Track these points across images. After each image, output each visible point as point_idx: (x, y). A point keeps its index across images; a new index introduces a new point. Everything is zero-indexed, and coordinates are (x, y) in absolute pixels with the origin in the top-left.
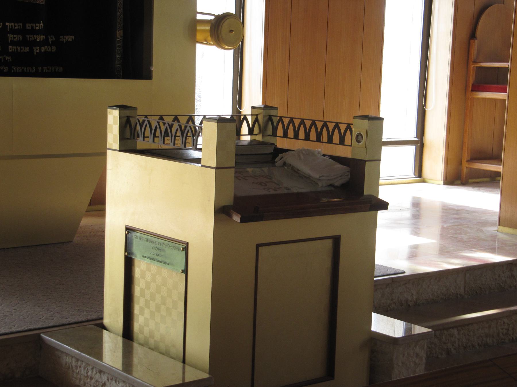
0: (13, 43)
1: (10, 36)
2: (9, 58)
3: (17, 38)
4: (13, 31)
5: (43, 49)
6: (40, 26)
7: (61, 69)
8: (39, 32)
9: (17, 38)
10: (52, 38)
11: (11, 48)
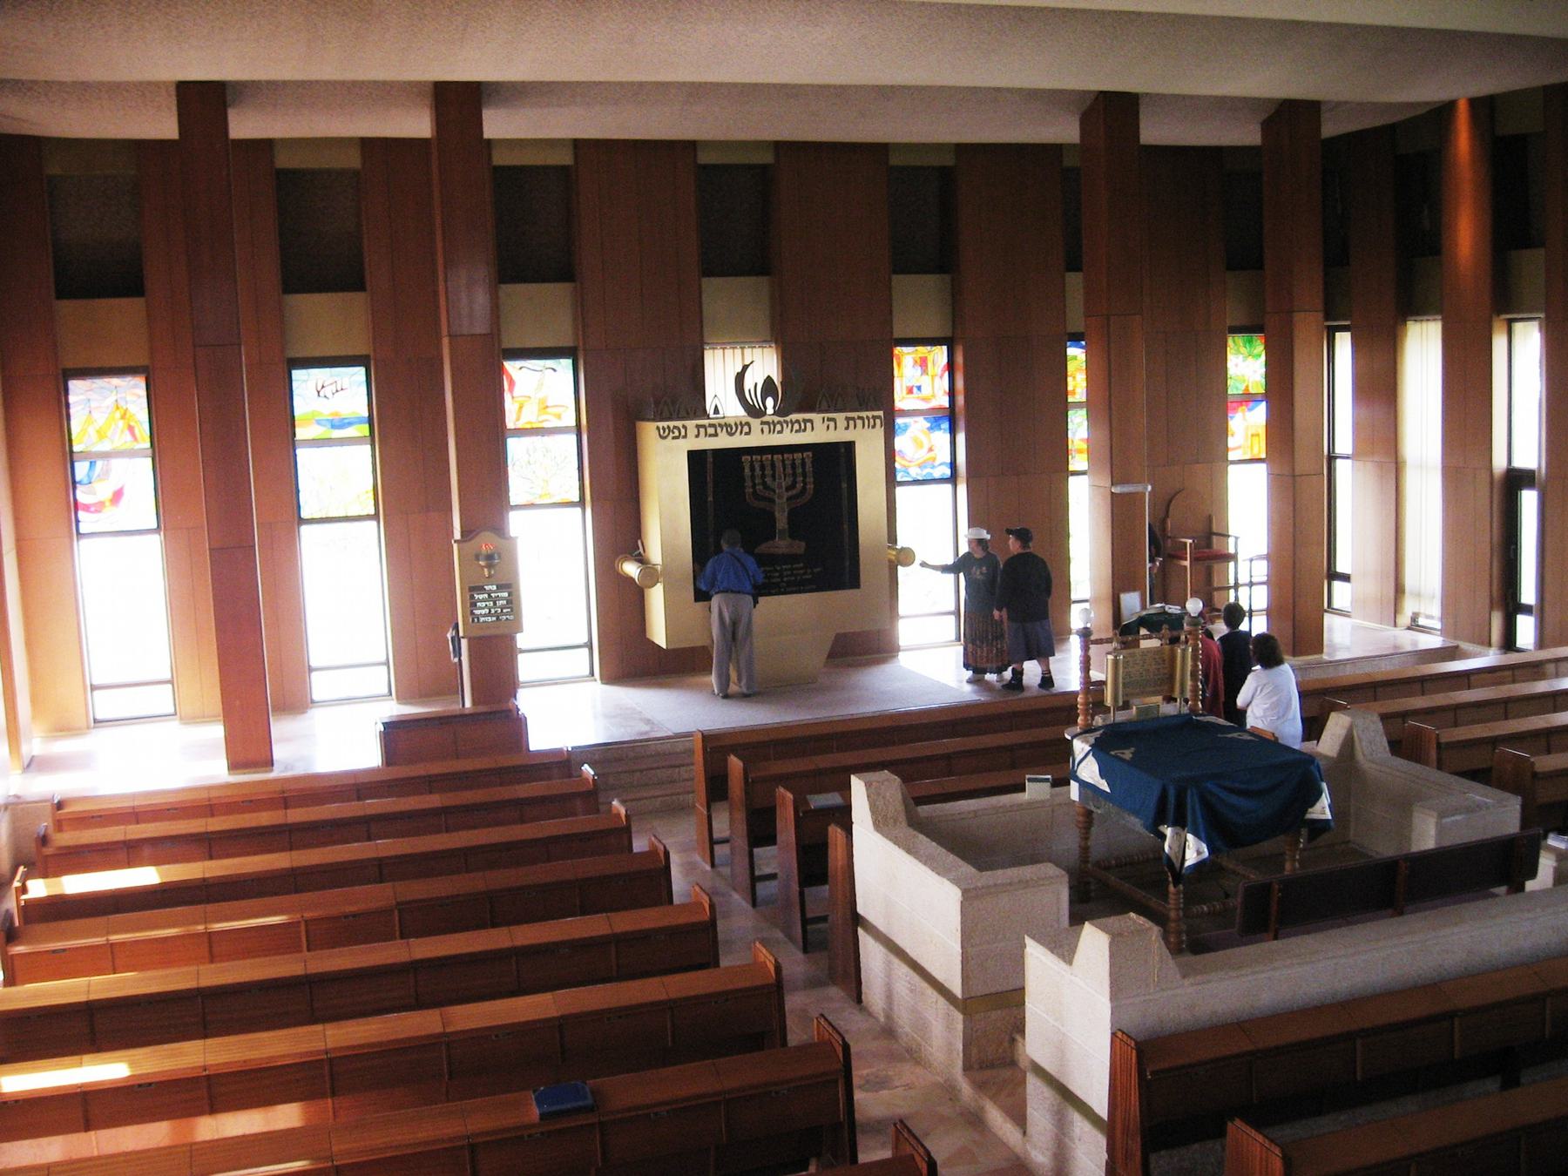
0: (787, 576)
1: (785, 573)
2: (784, 584)
3: (789, 573)
4: (786, 569)
5: (804, 577)
6: (802, 565)
7: (814, 587)
8: (801, 569)
9: (789, 573)
10: (809, 571)
11: (785, 579)
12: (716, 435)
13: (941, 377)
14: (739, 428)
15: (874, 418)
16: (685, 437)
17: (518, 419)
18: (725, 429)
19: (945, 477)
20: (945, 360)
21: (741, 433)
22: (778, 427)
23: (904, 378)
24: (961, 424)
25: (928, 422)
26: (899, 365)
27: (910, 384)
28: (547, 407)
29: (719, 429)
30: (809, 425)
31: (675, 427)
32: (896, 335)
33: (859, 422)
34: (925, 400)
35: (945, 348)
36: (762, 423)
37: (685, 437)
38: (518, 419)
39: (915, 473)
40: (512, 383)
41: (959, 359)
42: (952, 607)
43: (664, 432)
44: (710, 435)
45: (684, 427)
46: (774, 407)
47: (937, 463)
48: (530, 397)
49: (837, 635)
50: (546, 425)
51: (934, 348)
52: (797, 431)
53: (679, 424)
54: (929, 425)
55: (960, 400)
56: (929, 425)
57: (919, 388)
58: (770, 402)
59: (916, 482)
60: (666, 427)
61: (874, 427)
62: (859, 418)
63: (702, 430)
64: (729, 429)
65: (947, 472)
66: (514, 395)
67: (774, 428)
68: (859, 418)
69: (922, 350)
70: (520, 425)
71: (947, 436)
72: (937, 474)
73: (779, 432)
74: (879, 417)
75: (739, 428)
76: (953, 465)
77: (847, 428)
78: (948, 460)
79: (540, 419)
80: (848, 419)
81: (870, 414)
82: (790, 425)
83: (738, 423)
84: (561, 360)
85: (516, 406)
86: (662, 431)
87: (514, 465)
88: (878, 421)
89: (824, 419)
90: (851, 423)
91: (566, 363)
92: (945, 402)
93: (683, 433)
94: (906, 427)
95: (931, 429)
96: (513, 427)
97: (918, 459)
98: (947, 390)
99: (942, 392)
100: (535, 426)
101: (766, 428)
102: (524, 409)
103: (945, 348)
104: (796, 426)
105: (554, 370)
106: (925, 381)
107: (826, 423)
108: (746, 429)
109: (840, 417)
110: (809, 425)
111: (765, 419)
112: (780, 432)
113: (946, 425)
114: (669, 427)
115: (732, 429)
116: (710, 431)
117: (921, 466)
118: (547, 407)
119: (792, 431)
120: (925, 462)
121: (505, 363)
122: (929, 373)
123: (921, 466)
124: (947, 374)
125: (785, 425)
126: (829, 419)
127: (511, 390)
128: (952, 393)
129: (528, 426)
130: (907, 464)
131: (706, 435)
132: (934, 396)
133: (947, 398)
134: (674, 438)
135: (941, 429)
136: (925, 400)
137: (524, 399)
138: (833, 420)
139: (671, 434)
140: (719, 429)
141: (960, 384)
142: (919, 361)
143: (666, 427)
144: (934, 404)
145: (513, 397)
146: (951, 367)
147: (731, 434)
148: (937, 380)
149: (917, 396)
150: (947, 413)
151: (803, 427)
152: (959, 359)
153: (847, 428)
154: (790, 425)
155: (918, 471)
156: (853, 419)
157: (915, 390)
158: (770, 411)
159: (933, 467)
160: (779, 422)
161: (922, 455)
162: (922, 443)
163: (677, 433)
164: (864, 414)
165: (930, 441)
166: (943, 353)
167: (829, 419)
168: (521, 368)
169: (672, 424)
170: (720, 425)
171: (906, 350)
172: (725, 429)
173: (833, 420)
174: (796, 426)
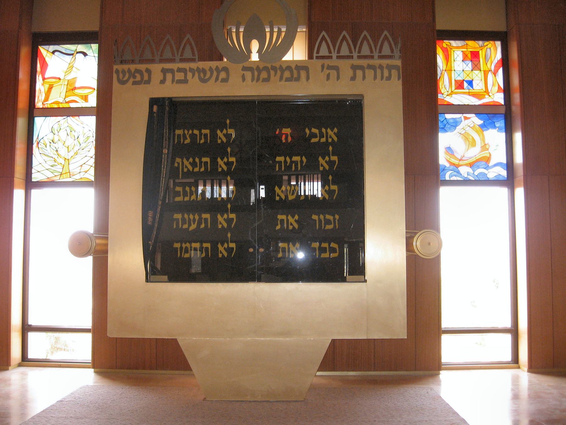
12: (185, 81)
13: (495, 73)
14: (215, 74)
15: (390, 68)
16: (148, 82)
17: (47, 99)
18: (197, 74)
19: (501, 178)
20: (499, 56)
21: (217, 79)
22: (264, 75)
23: (453, 72)
24: (518, 123)
25: (481, 119)
26: (447, 58)
27: (460, 78)
28: (75, 88)
29: (190, 75)
30: (303, 74)
31: (137, 71)
32: (441, 25)
33: (370, 73)
34: (477, 95)
35: (498, 44)
36: (245, 69)
37: (148, 82)
38: (47, 99)
39: (465, 171)
40: (45, 65)
41: (514, 55)
42: (508, 324)
43: (124, 77)
44: (179, 82)
45: (149, 71)
46: (259, 52)
47: (491, 164)
48: (60, 79)
49: (333, 341)
50: (73, 105)
51: (486, 43)
52: (287, 80)
53: (142, 67)
54: (481, 122)
55: (516, 98)
56: (481, 122)
57: (470, 83)
58: (255, 45)
59: (466, 182)
60: (126, 70)
61: (389, 78)
62: (370, 67)
63: (169, 76)
64: (202, 75)
65: (504, 173)
66: (46, 76)
67: (259, 76)
68: (370, 67)
69: (473, 45)
70: (48, 105)
71: (502, 136)
72: (492, 174)
73: (265, 80)
74: (395, 67)
75: (215, 74)
76: (510, 165)
77: (353, 78)
78: (504, 160)
79: (67, 100)
80: (355, 68)
81: (385, 62)
82: (279, 73)
83: (214, 68)
84: (92, 45)
85: (47, 86)
86: (121, 76)
87: (38, 143)
88: (394, 73)
89: (323, 66)
90: (359, 73)
91: (93, 50)
92: (499, 98)
93: (146, 77)
94: (455, 124)
95: (483, 127)
96: (41, 107)
97: (470, 158)
98: (502, 86)
99: (496, 88)
100: (61, 106)
101: (248, 74)
102: (53, 90)
103: (498, 44)
104: (287, 74)
105: (85, 54)
106: (477, 77)
107: (327, 72)
108: (223, 75)
109: (345, 66)
110: (303, 74)
111: (246, 64)
112: (267, 80)
113: (501, 123)
114: (129, 70)
115: (205, 75)
116: (180, 76)
117: (471, 165)
118: (75, 88)
119: (281, 79)
120: (478, 161)
121: (39, 47)
122: (482, 69)
123: (471, 165)
124: (501, 71)
125: (272, 73)
126: (329, 67)
127: (43, 73)
128: (507, 90)
129: (55, 106)
130: (456, 162)
131: (173, 81)
132: (487, 92)
133: (501, 95)
134: (135, 83)
135: (495, 127)
136: (477, 95)
137: (54, 80)
138: (336, 68)
139: (132, 80)
140: (190, 75)
141: (515, 81)
142: (469, 55)
143: (126, 70)
144: (487, 100)
145: (44, 79)
146: (505, 63)
147: (203, 81)
148: (490, 76)
149: (468, 91)
150: (503, 110)
151: (295, 75)
152: (514, 55)
153: (353, 78)
154: (279, 73)
155: (470, 170)
156: (362, 68)
157: (466, 85)
158: (255, 57)
159: (487, 168)
160: (266, 68)
161: (474, 153)
162: (473, 139)
163: (138, 78)
164: (376, 62)
165: (484, 141)
166: (496, 49)
167: (329, 67)
168: (53, 52)
169: (133, 67)
170: (191, 70)
171: (454, 43)
172: (197, 74)
173: (336, 68)
174: (287, 74)
